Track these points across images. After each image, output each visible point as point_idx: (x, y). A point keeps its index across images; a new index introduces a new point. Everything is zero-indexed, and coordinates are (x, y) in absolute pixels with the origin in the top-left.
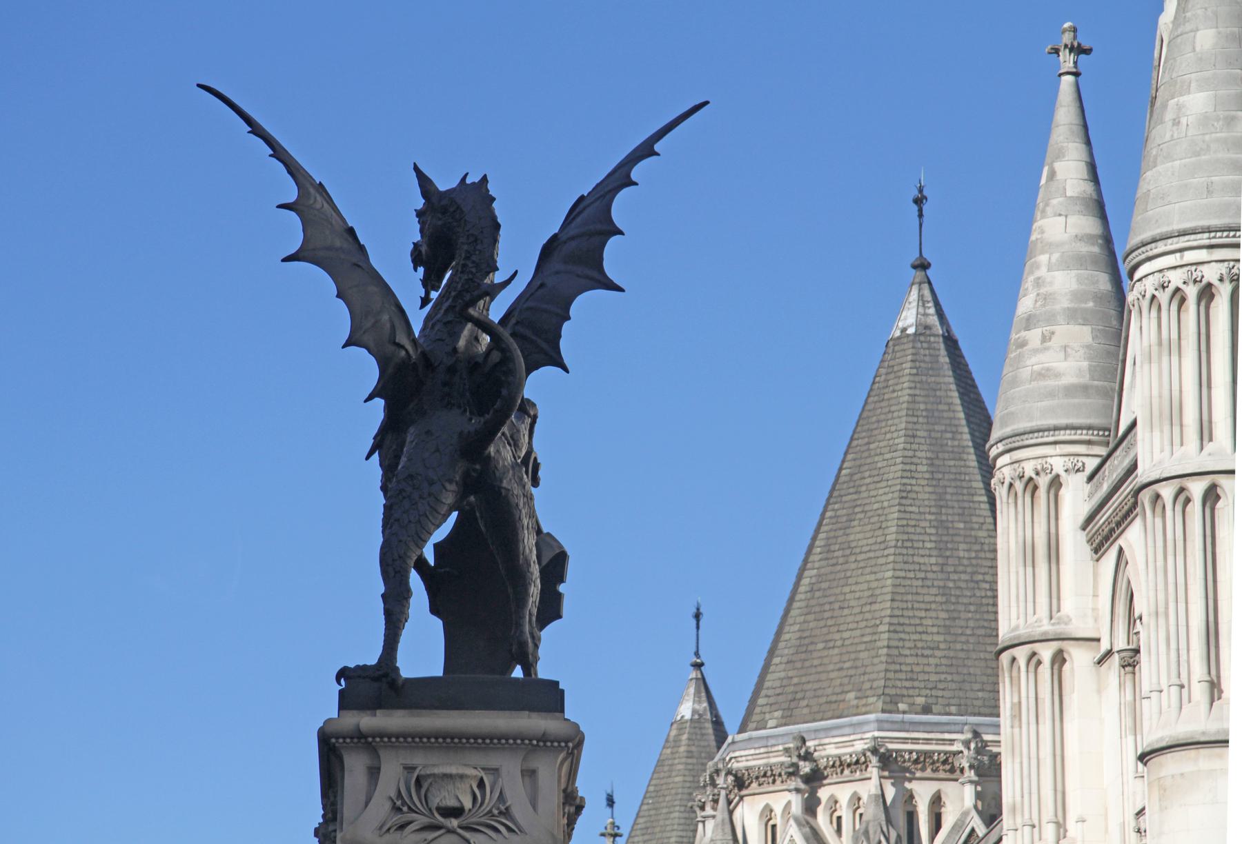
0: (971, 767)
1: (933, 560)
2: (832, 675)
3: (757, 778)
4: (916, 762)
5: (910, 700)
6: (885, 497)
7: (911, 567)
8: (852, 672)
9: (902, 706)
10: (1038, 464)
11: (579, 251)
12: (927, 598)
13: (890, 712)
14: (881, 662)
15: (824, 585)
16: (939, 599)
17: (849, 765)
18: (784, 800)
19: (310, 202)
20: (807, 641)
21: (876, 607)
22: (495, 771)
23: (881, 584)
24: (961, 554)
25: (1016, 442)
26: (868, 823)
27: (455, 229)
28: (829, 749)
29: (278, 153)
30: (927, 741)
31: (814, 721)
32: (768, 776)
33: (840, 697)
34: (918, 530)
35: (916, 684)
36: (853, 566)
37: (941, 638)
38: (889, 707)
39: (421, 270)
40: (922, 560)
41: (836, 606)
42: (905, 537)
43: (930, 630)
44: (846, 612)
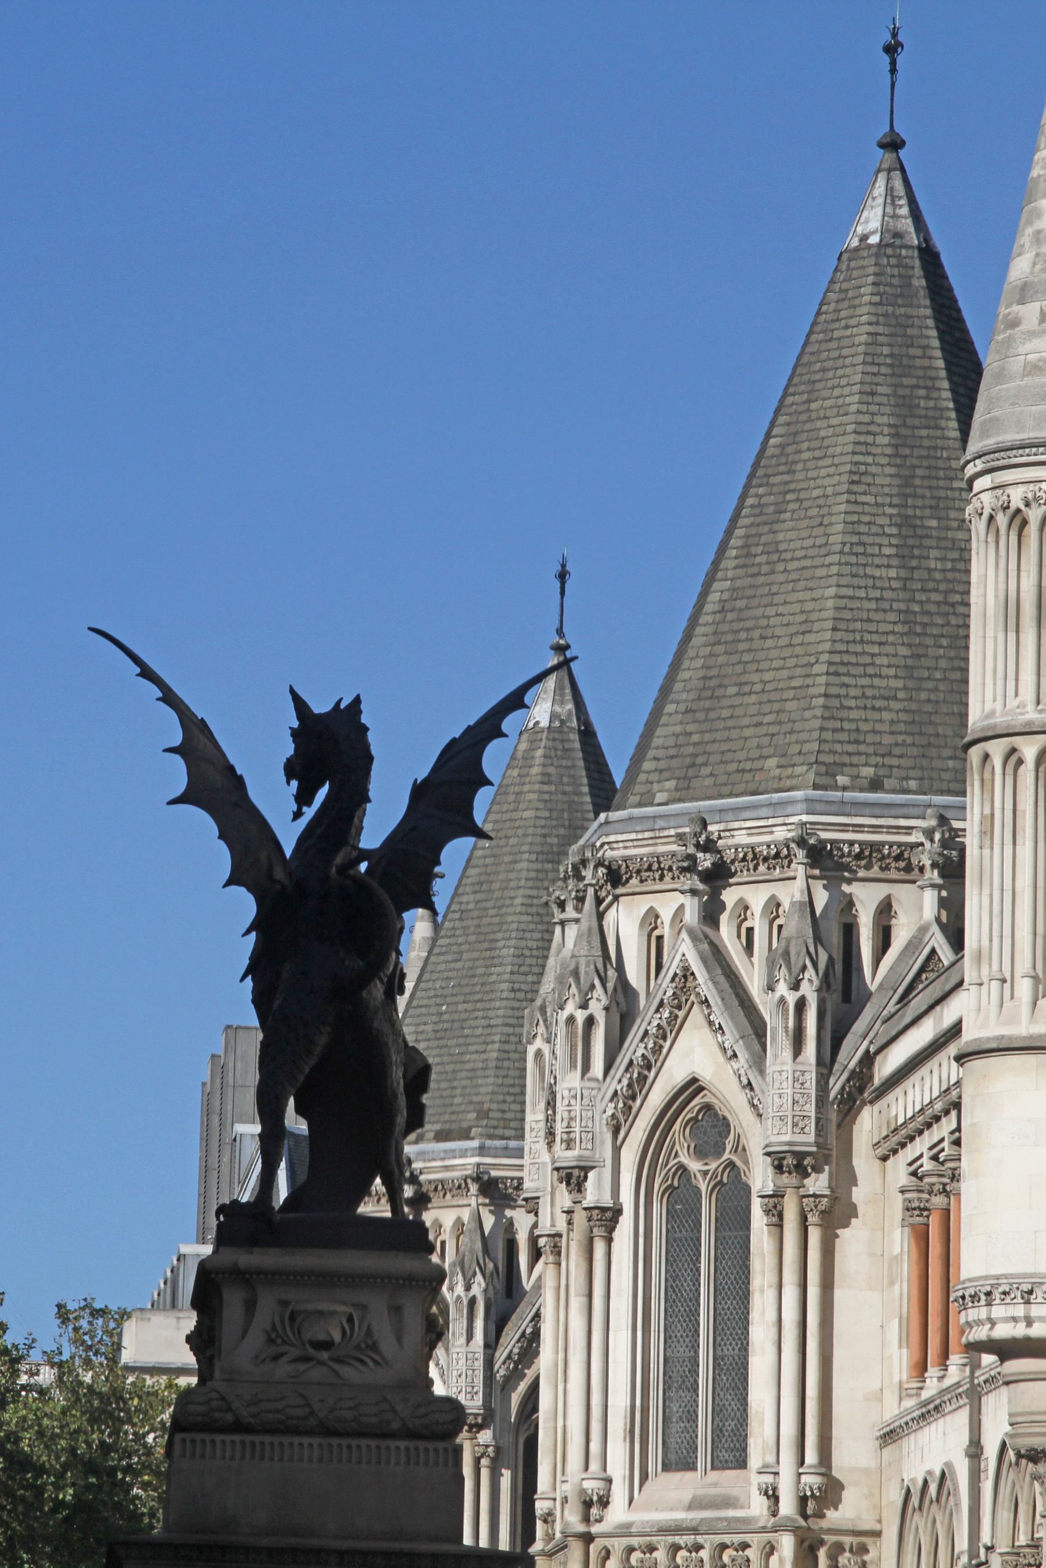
0: (934, 865)
1: (893, 573)
2: (747, 732)
3: (639, 872)
4: (859, 856)
5: (854, 771)
6: (827, 481)
7: (862, 582)
8: (773, 729)
9: (841, 780)
10: (1028, 491)
11: (448, 796)
12: (883, 627)
13: (825, 788)
14: (815, 717)
15: (740, 604)
16: (898, 628)
17: (766, 859)
18: (675, 904)
19: (197, 745)
20: (713, 683)
21: (809, 638)
22: (363, 1307)
23: (818, 605)
24: (932, 565)
25: (1002, 456)
26: (788, 940)
27: (330, 749)
28: (739, 836)
29: (169, 698)
30: (875, 829)
31: (721, 796)
32: (654, 870)
33: (757, 764)
34: (874, 529)
35: (863, 748)
36: (781, 578)
37: (900, 684)
38: (823, 780)
39: (294, 784)
40: (877, 573)
41: (756, 634)
42: (855, 539)
43: (885, 671)
44: (769, 643)
